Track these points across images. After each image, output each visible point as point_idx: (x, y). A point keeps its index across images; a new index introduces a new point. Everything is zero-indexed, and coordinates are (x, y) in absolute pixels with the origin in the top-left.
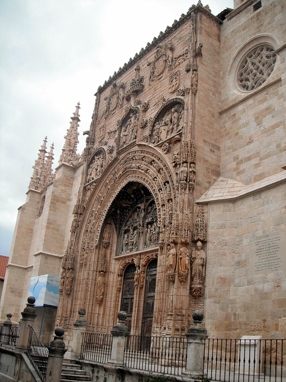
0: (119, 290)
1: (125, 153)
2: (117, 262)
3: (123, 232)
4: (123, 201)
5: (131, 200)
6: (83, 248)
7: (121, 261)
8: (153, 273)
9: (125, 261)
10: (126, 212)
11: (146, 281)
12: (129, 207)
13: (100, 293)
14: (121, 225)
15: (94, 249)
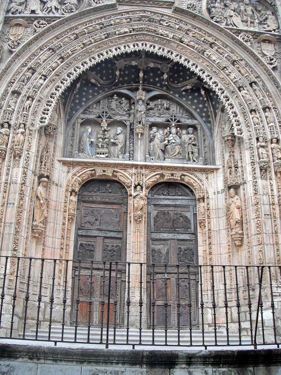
0: (71, 220)
1: (134, 7)
2: (65, 168)
3: (80, 121)
4: (92, 73)
5: (104, 78)
6: (8, 123)
7: (78, 168)
8: (162, 203)
9: (94, 170)
10: (87, 92)
11: (149, 214)
12: (97, 86)
13: (40, 219)
14: (74, 109)
15: (35, 131)
